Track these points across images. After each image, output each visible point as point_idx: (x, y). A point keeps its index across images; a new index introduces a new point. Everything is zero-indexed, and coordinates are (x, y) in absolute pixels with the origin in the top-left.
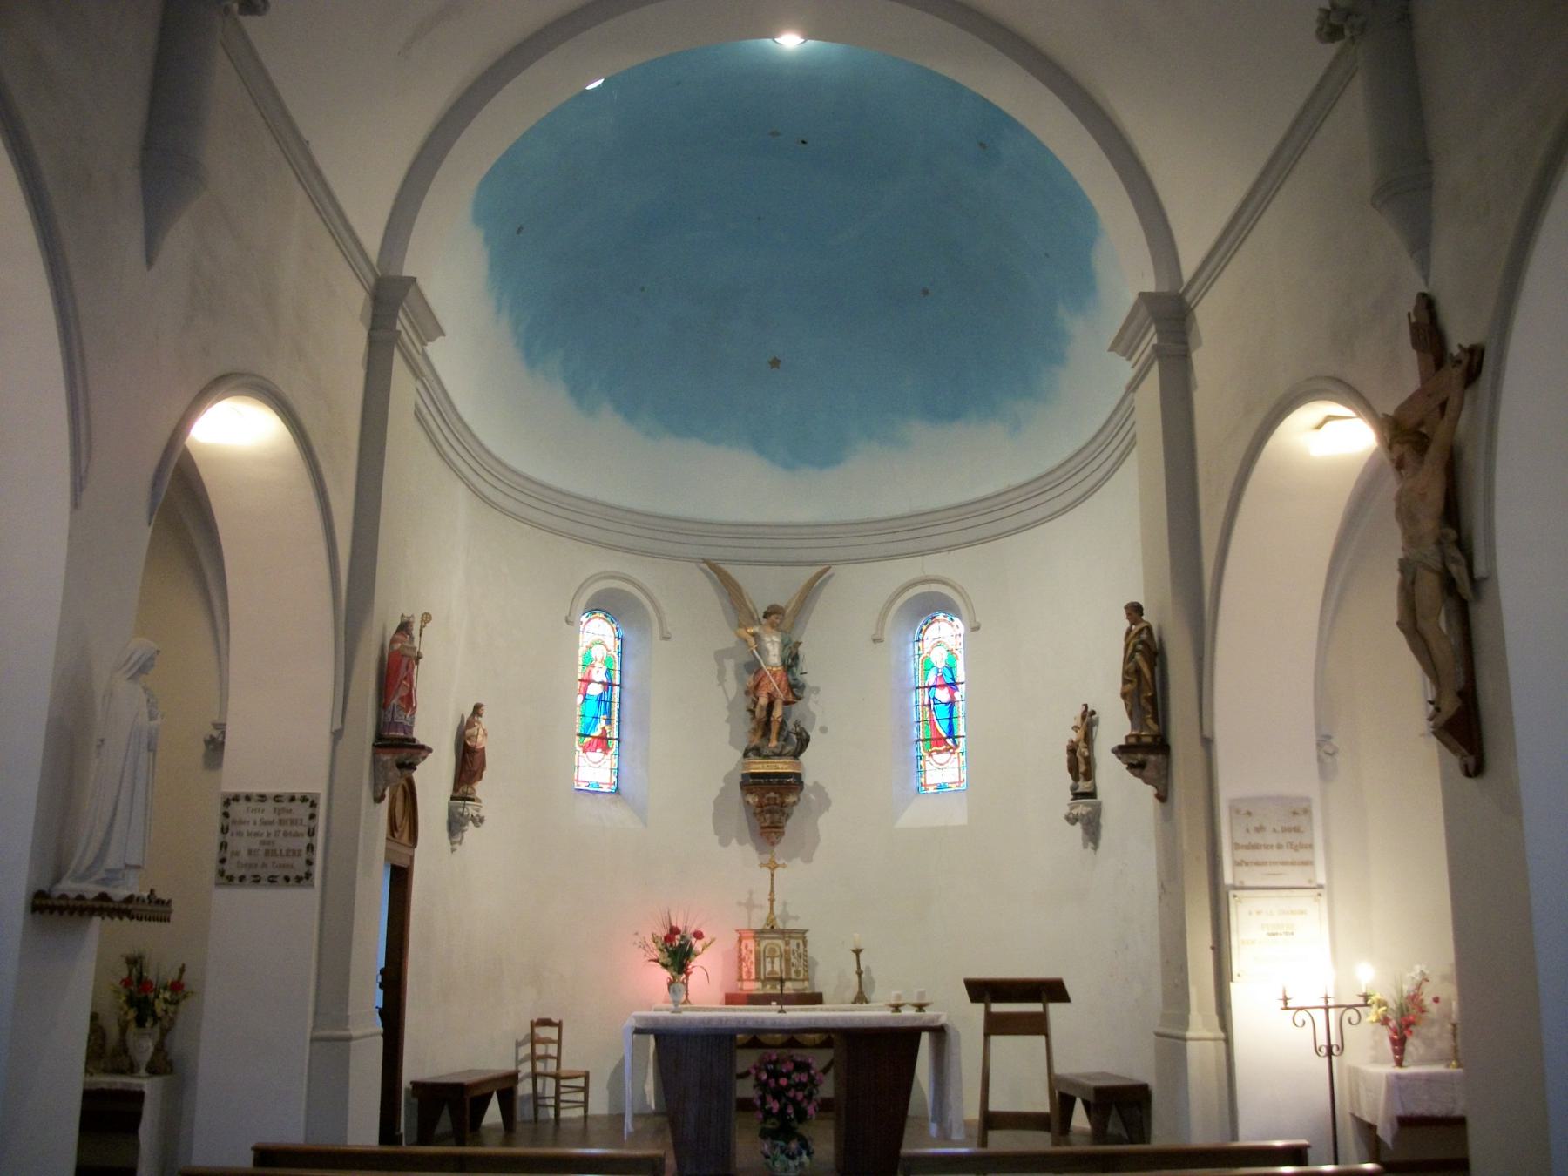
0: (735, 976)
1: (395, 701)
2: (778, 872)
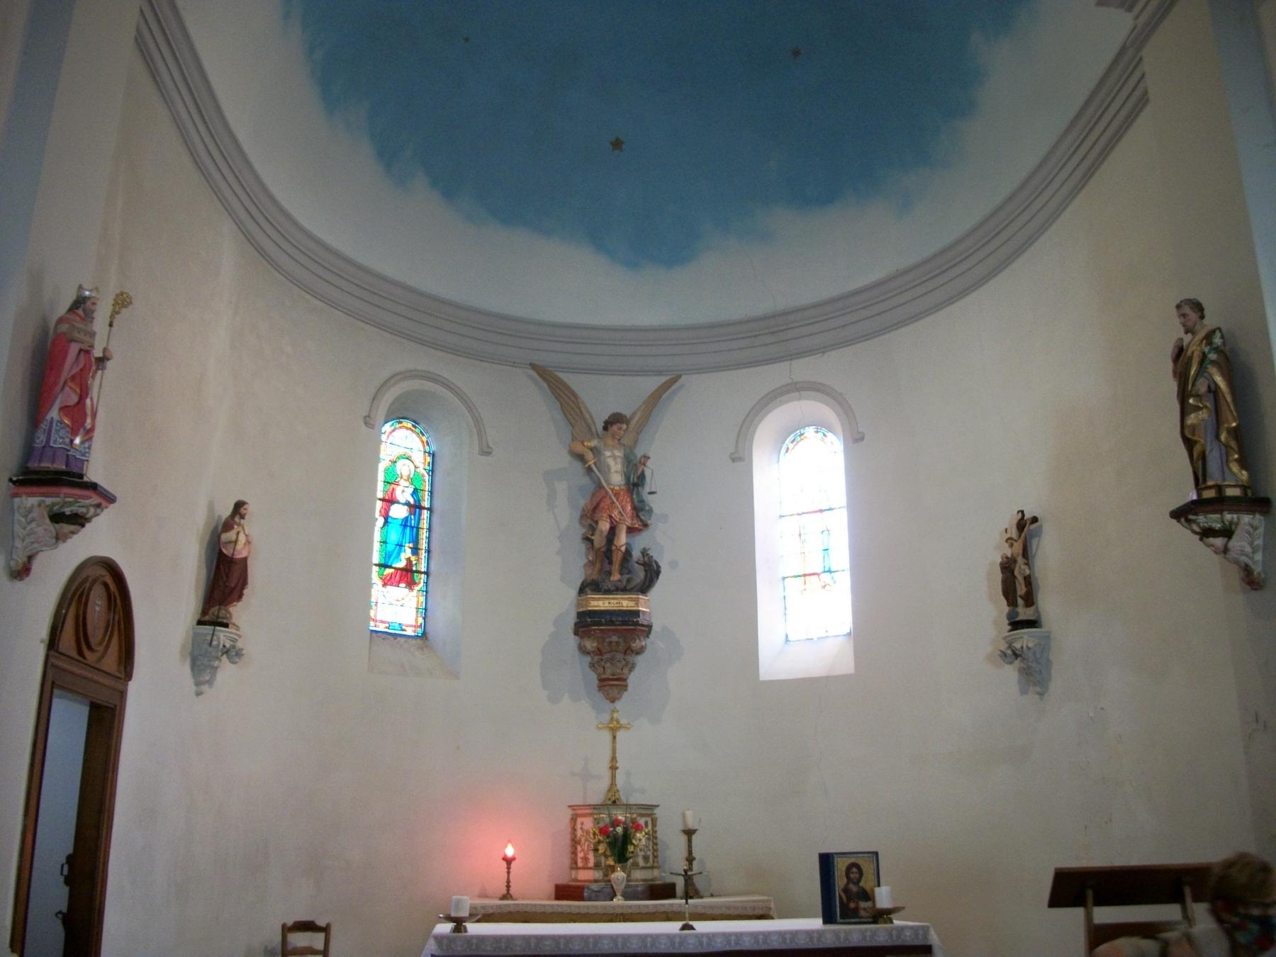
0: (566, 861)
1: (54, 414)
2: (620, 735)
